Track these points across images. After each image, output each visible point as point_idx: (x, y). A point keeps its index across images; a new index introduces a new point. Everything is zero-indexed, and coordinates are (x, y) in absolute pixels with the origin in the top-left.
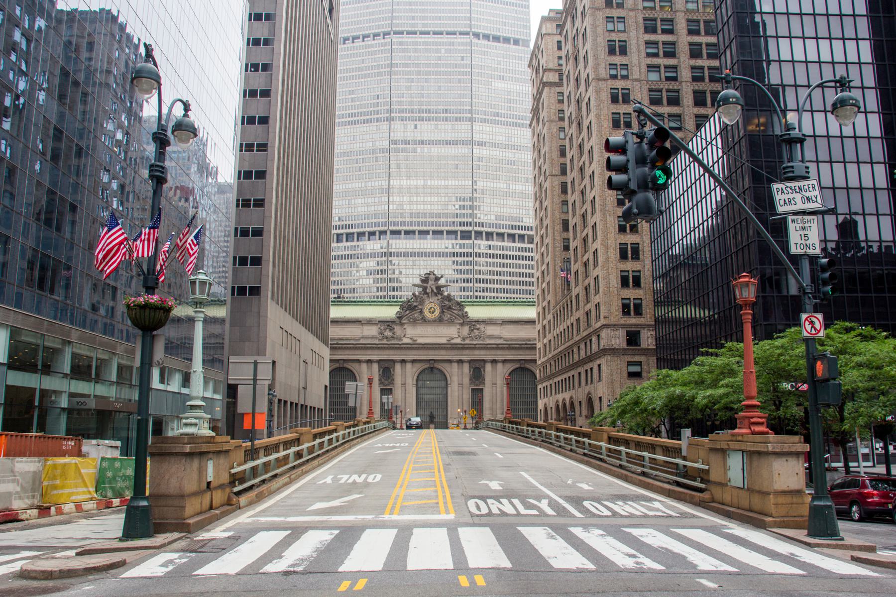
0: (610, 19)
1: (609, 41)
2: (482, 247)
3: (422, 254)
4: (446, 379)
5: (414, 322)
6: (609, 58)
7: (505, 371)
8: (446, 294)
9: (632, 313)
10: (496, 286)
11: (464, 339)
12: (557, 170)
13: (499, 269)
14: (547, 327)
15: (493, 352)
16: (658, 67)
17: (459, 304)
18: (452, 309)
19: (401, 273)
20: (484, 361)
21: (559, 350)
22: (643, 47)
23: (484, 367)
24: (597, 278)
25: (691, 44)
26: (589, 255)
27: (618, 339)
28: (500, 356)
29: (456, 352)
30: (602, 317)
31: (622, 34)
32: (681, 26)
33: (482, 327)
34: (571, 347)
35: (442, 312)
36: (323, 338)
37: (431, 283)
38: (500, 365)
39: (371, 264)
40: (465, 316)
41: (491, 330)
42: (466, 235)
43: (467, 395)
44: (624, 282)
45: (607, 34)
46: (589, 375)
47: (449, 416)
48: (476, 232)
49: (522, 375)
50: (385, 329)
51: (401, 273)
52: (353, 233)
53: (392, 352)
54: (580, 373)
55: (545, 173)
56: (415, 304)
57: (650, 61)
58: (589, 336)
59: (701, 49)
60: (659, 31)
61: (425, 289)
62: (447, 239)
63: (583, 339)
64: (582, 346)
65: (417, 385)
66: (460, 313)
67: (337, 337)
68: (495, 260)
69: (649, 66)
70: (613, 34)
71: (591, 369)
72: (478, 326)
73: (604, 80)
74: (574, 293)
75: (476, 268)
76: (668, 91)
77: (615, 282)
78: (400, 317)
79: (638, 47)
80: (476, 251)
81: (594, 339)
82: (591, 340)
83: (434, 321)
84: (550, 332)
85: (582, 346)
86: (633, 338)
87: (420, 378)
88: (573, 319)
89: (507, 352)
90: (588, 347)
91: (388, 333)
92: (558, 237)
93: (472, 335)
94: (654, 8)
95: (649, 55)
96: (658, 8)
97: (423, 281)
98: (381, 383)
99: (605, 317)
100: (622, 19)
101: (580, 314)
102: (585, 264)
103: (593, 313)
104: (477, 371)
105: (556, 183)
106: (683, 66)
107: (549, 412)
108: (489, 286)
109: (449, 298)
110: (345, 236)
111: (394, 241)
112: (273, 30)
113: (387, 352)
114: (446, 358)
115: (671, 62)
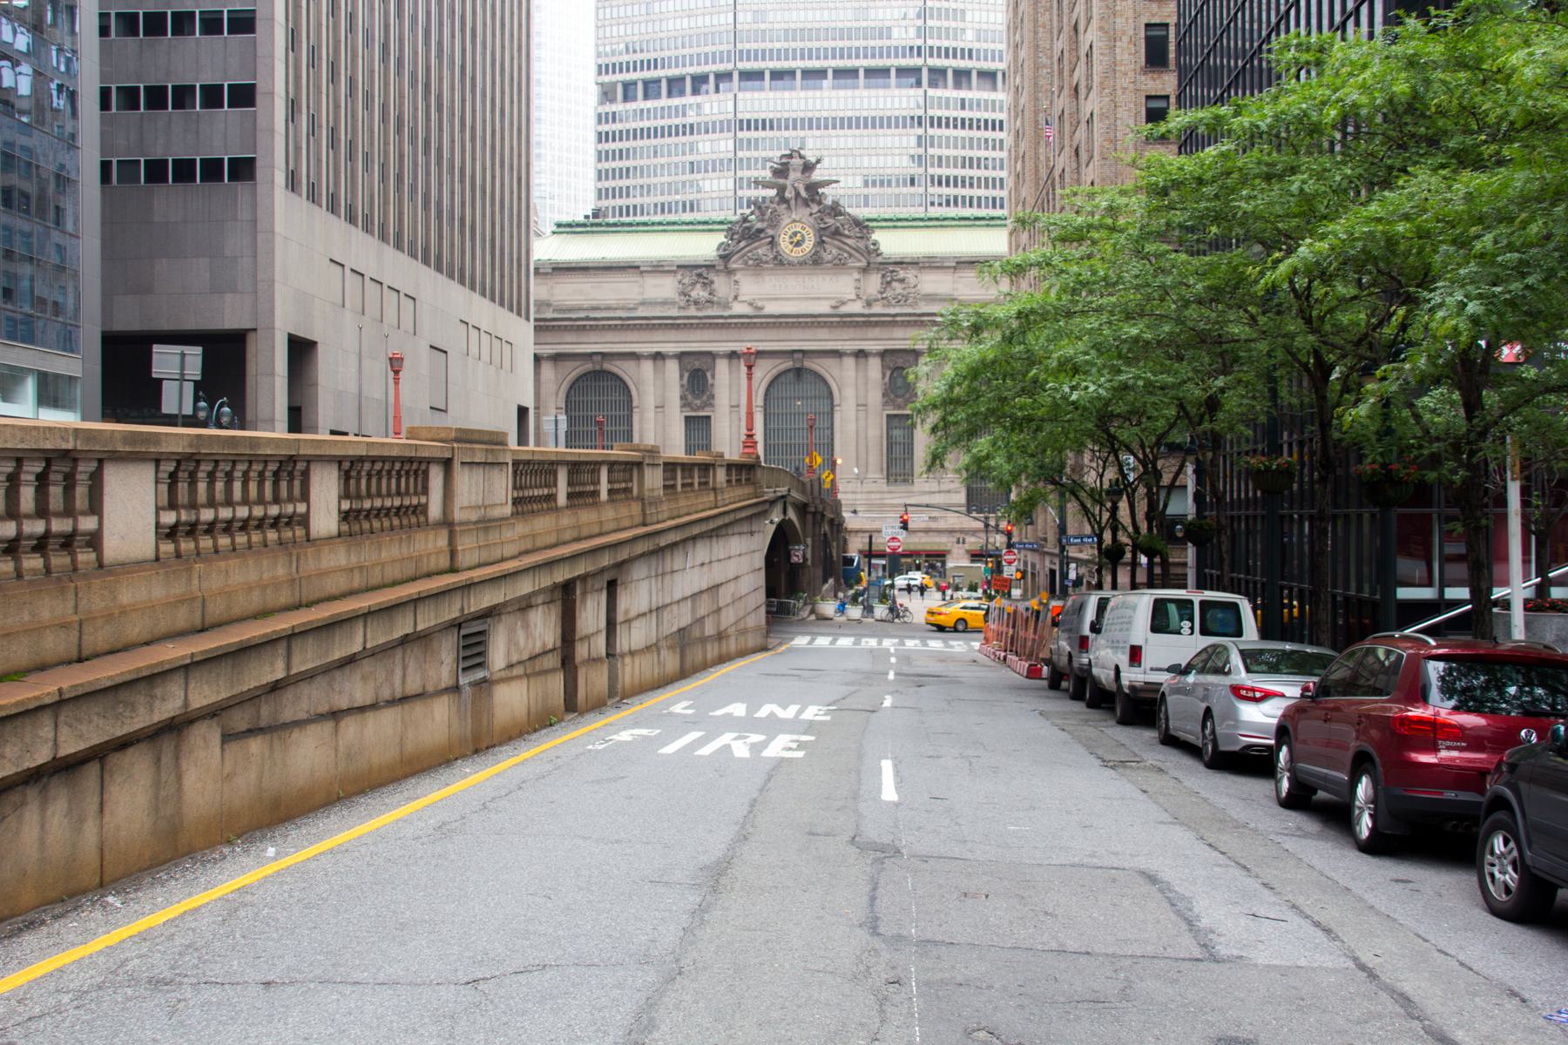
4: (831, 393)
5: (758, 266)
10: (976, 192)
11: (869, 304)
17: (858, 223)
33: (909, 274)
35: (820, 243)
37: (794, 175)
40: (873, 251)
41: (931, 283)
42: (909, 74)
43: (876, 429)
48: (932, 70)
50: (693, 284)
52: (658, 81)
56: (759, 225)
62: (867, 87)
66: (861, 244)
67: (586, 304)
72: (902, 274)
75: (931, 151)
78: (725, 258)
83: (802, 263)
91: (699, 293)
98: (685, 404)
108: (960, 191)
109: (835, 210)
110: (640, 87)
111: (748, 95)
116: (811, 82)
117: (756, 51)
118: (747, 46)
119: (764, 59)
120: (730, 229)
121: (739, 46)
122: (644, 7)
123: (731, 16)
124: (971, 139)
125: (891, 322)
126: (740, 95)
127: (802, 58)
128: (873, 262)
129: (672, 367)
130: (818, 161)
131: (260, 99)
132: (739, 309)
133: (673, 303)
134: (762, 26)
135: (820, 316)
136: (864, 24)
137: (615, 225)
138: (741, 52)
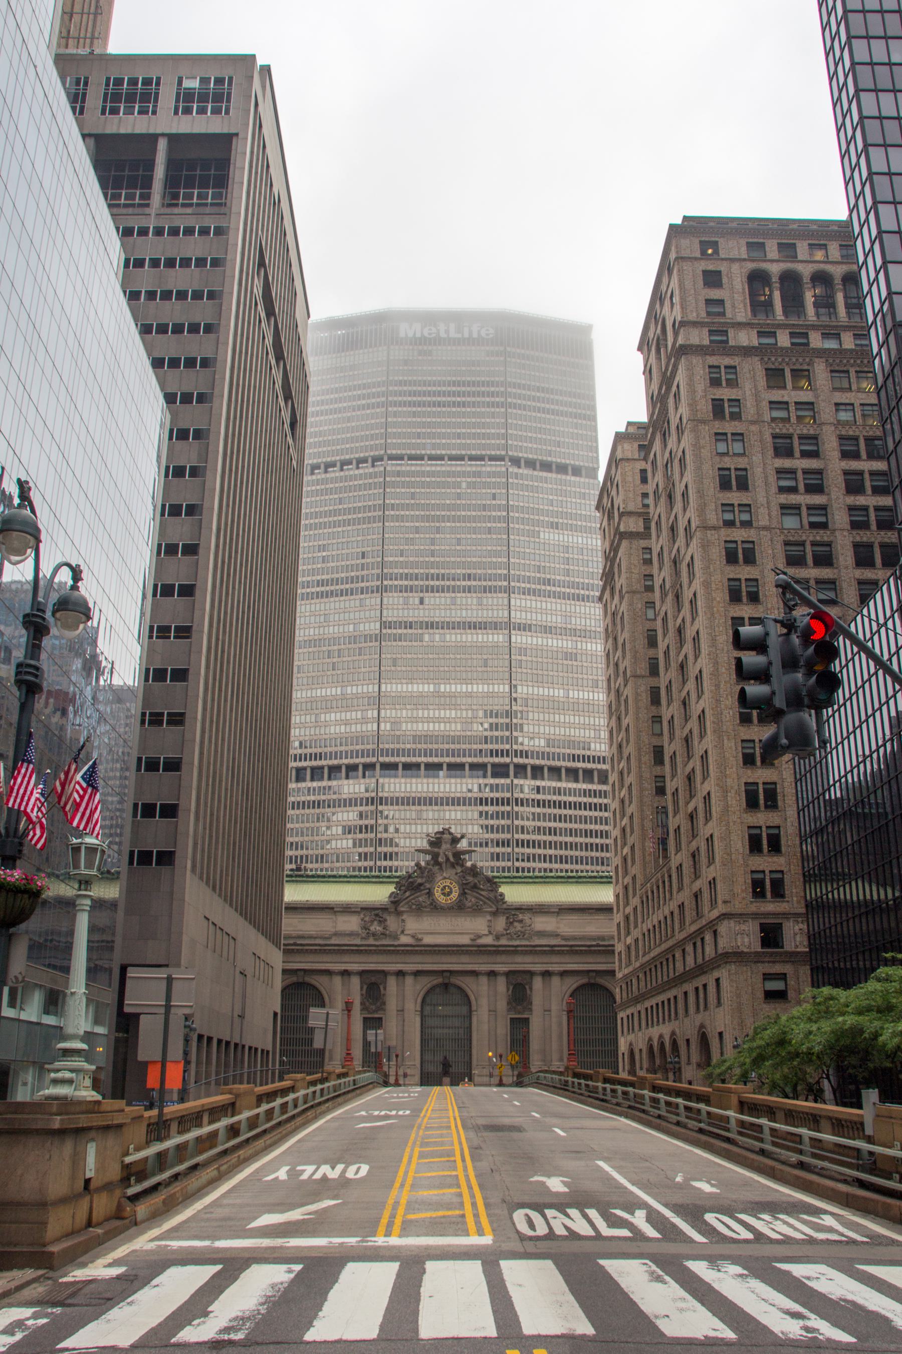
0: (720, 436)
1: (719, 469)
2: (526, 790)
3: (430, 801)
4: (470, 1003)
5: (419, 910)
6: (721, 495)
7: (565, 988)
8: (469, 864)
9: (769, 894)
11: (498, 938)
12: (643, 668)
13: (552, 824)
14: (632, 918)
15: (546, 959)
16: (797, 507)
17: (489, 880)
18: (479, 891)
19: (397, 830)
20: (531, 974)
21: (652, 955)
22: (772, 478)
23: (530, 984)
24: (710, 839)
25: (846, 473)
26: (697, 802)
27: (748, 937)
28: (556, 965)
29: (485, 958)
30: (720, 902)
31: (740, 459)
32: (830, 445)
33: (526, 917)
34: (671, 949)
35: (463, 894)
36: (273, 935)
37: (445, 846)
38: (556, 980)
39: (349, 816)
41: (542, 923)
42: (500, 771)
43: (503, 1029)
44: (755, 845)
45: (718, 459)
46: (701, 995)
47: (474, 1062)
49: (593, 996)
50: (372, 922)
51: (397, 830)
52: (322, 768)
53: (381, 958)
54: (686, 993)
55: (625, 672)
56: (419, 881)
57: (784, 499)
58: (700, 931)
59: (862, 480)
60: (797, 454)
61: (435, 856)
62: (471, 777)
63: (691, 937)
64: (689, 948)
65: (422, 1011)
66: (492, 895)
67: (294, 933)
68: (547, 811)
69: (783, 507)
70: (726, 459)
71: (705, 986)
73: (714, 528)
74: (674, 864)
75: (516, 822)
76: (813, 544)
77: (740, 844)
78: (395, 901)
79: (766, 477)
80: (516, 795)
81: (708, 937)
82: (702, 939)
84: (636, 927)
85: (689, 948)
86: (771, 935)
87: (428, 1000)
88: (673, 905)
89: (567, 959)
90: (699, 950)
91: (376, 927)
92: (646, 775)
93: (512, 930)
94: (788, 420)
95: (782, 490)
96: (793, 419)
97: (431, 843)
98: (364, 1008)
99: (725, 902)
100: (739, 436)
101: (685, 896)
102: (692, 817)
103: (706, 895)
104: (520, 990)
105: (643, 688)
106: (835, 505)
107: (637, 1057)
108: (538, 851)
109: (474, 871)
111: (387, 780)
112: (205, 455)
113: (375, 958)
114: (469, 967)
115: (818, 499)
116: (431, 772)
117: (393, 750)
118: (387, 746)
119: (398, 756)
120: (397, 883)
121: (381, 746)
122: (313, 717)
123: (375, 725)
124: (544, 815)
125: (514, 951)
126: (381, 780)
127: (425, 756)
128: (500, 907)
129: (356, 981)
130: (463, 837)
131: (180, 813)
132: (404, 940)
133: (357, 935)
134: (398, 733)
135: (463, 946)
136: (469, 733)
137: (313, 876)
138: (382, 750)
